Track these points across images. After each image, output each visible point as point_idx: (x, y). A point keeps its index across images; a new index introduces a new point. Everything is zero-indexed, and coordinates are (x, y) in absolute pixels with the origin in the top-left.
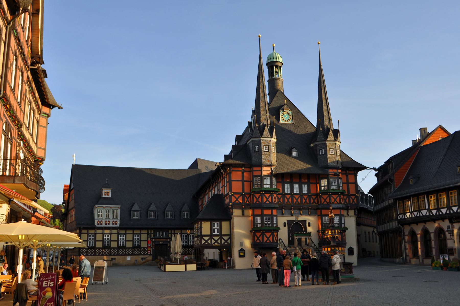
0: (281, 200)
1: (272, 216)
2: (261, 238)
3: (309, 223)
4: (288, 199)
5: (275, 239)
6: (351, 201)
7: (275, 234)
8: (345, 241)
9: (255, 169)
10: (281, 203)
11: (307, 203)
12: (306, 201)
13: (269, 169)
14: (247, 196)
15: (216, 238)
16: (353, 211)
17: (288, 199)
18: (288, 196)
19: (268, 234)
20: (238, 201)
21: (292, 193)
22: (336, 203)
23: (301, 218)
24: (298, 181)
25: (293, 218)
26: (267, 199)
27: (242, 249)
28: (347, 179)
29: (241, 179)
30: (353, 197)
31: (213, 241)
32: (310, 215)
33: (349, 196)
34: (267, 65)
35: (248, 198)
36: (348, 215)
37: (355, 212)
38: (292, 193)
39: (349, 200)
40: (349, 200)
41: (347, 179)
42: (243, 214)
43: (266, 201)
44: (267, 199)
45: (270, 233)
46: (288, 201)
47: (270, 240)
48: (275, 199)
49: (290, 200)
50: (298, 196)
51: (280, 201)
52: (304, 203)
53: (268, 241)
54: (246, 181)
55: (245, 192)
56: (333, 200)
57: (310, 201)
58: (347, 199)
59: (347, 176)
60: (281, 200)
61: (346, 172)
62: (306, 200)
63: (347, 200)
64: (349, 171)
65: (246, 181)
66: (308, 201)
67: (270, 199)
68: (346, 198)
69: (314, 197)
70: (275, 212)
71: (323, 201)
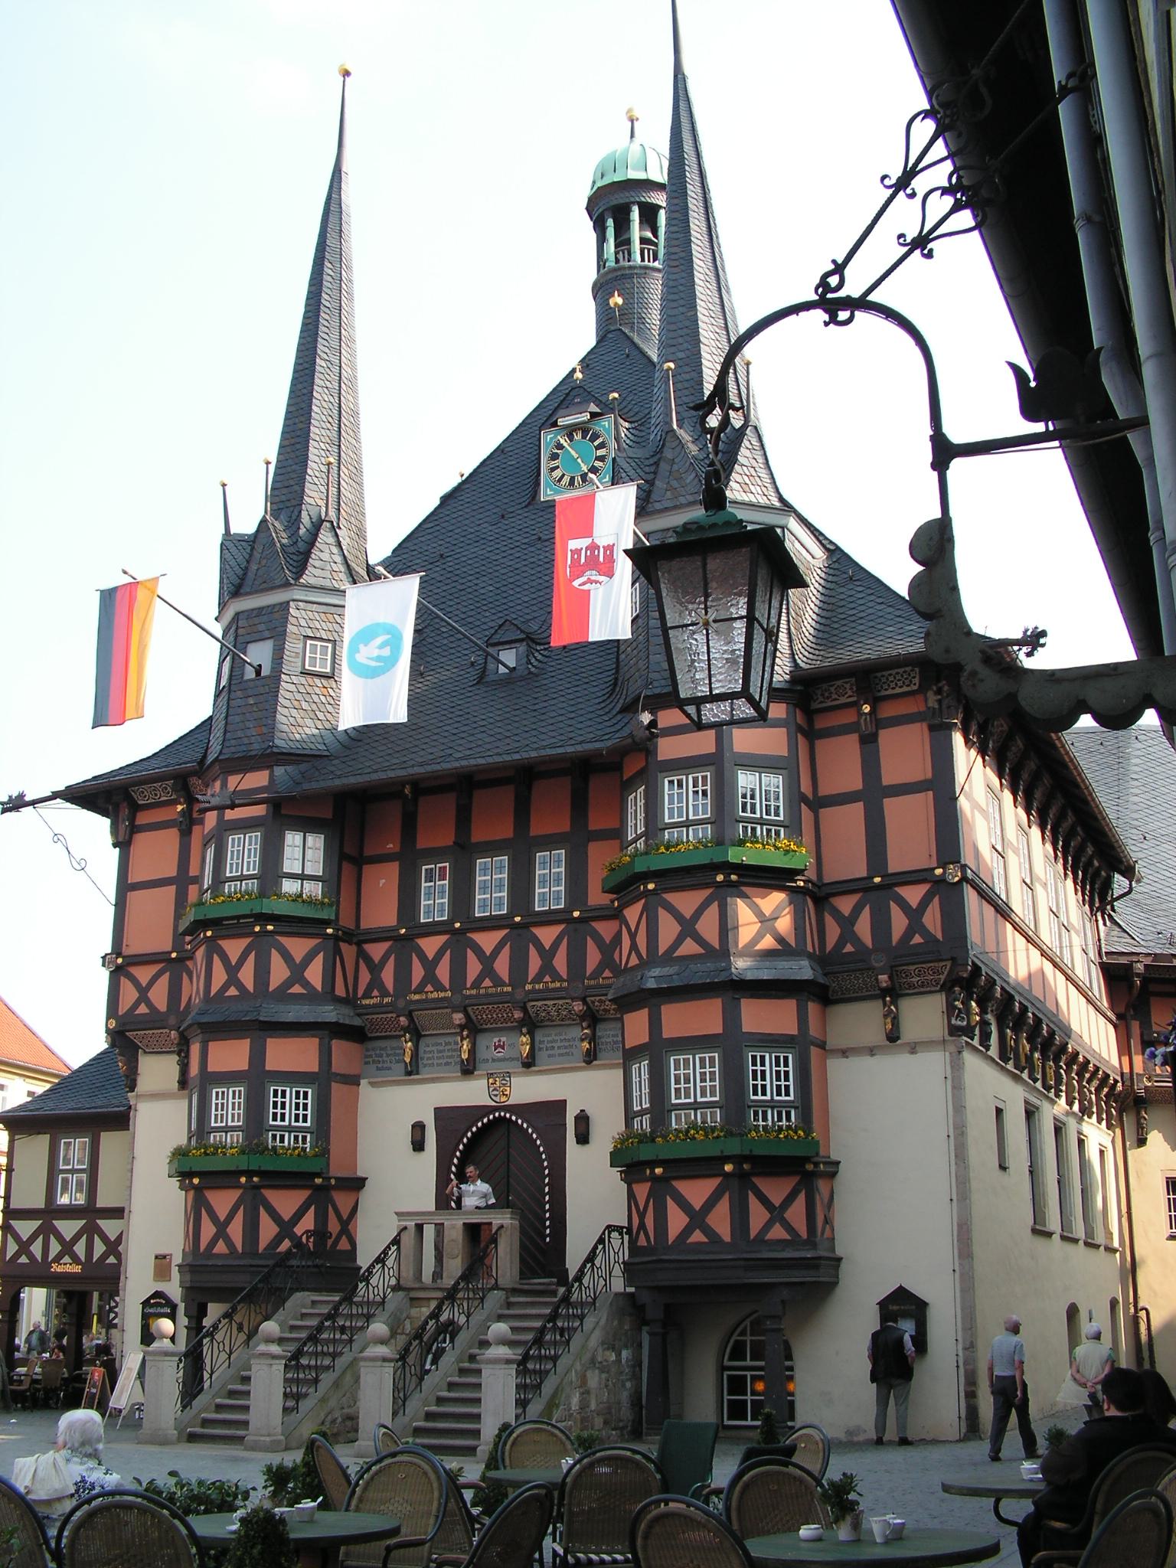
0: (388, 976)
1: (257, 1081)
3: (583, 1119)
4: (430, 966)
5: (268, 1230)
6: (899, 922)
7: (287, 1202)
8: (811, 1242)
10: (384, 993)
11: (556, 977)
12: (547, 968)
15: (68, 1228)
16: (938, 1001)
17: (430, 966)
18: (430, 945)
19: (223, 1201)
20: (149, 1004)
21: (462, 926)
22: (689, 947)
23: (527, 1089)
24: (505, 830)
25: (473, 1093)
26: (232, 970)
27: (157, 1294)
28: (871, 766)
30: (913, 895)
31: (55, 1248)
32: (590, 1058)
33: (879, 887)
36: (893, 1037)
37: (950, 1009)
38: (462, 926)
39: (880, 924)
40: (880, 924)
41: (871, 766)
42: (183, 1083)
43: (225, 987)
44: (232, 970)
45: (233, 1195)
46: (430, 977)
47: (229, 1243)
49: (443, 972)
50: (500, 934)
51: (376, 983)
52: (538, 979)
53: (221, 1247)
57: (576, 960)
58: (866, 913)
59: (869, 741)
60: (388, 976)
61: (860, 714)
62: (547, 955)
63: (863, 927)
64: (875, 702)
66: (560, 962)
67: (247, 976)
70: (291, 1054)
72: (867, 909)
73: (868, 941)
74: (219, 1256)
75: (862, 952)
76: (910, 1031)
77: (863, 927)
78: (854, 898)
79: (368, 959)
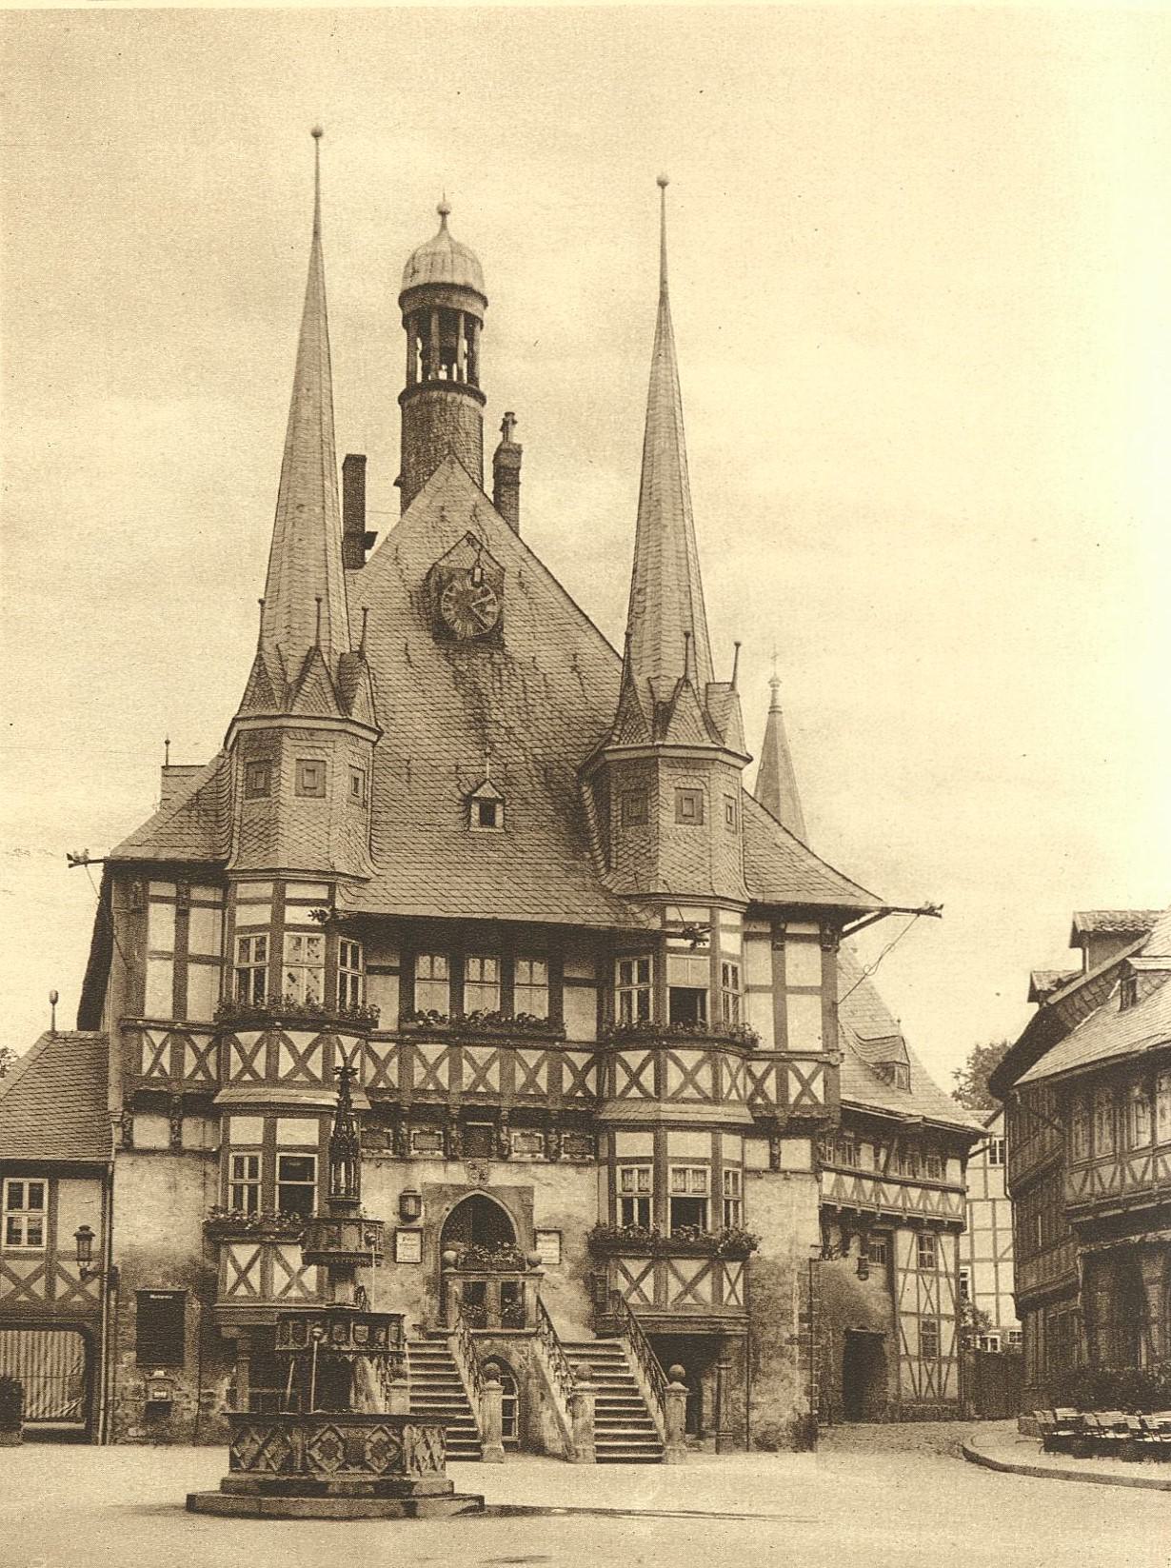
2: (254, 1277)
6: (795, 1088)
9: (243, 891)
12: (531, 1082)
13: (322, 893)
14: (202, 1042)
22: (690, 1092)
29: (171, 949)
30: (806, 1068)
33: (783, 1059)
35: (202, 1057)
39: (782, 1086)
40: (782, 1086)
53: (294, 1293)
54: (199, 960)
55: (190, 1018)
56: (674, 1079)
63: (771, 1085)
65: (199, 960)
68: (767, 1073)
69: (580, 1059)
71: (622, 1081)
72: (773, 1073)
73: (773, 1097)
74: (289, 1300)
75: (768, 1105)
76: (785, 1164)
77: (771, 1085)
78: (765, 1065)
79: (374, 1057)
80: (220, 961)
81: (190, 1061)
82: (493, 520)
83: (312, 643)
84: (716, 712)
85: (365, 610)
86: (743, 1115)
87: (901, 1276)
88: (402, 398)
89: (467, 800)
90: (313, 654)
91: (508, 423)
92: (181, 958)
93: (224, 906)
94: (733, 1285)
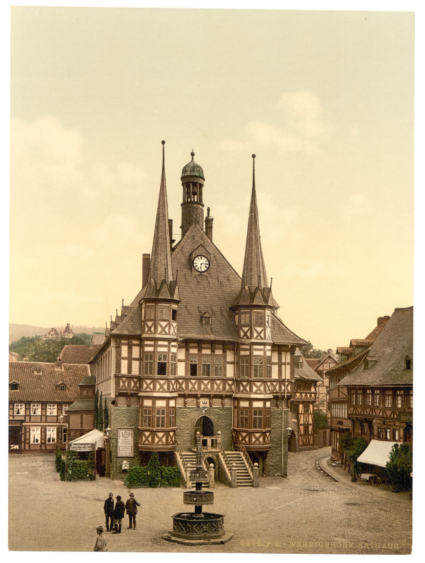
5: (170, 439)
9: (146, 343)
33: (281, 382)
34: (182, 179)
39: (280, 388)
47: (162, 442)
48: (173, 386)
68: (276, 385)
80: (140, 360)
81: (133, 384)
82: (205, 236)
83: (164, 279)
84: (266, 295)
85: (177, 271)
86: (271, 396)
87: (300, 415)
88: (182, 205)
89: (202, 317)
90: (164, 282)
91: (208, 209)
92: (130, 359)
93: (141, 346)
94: (268, 438)
